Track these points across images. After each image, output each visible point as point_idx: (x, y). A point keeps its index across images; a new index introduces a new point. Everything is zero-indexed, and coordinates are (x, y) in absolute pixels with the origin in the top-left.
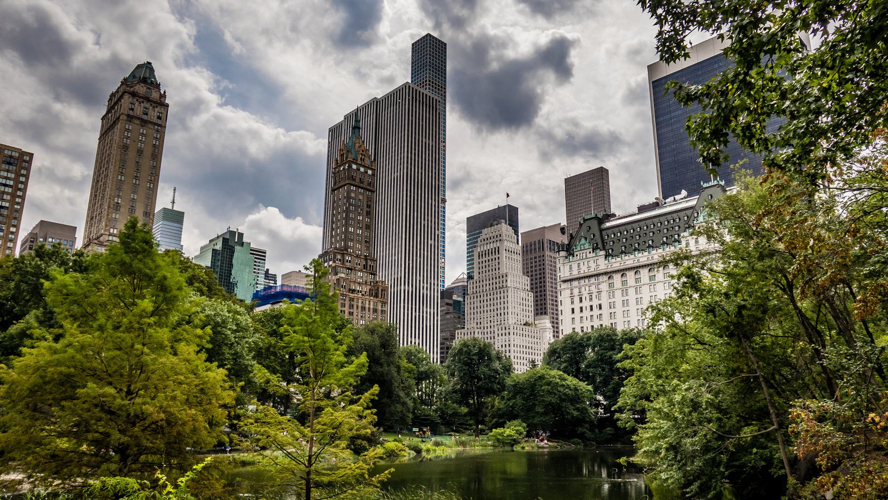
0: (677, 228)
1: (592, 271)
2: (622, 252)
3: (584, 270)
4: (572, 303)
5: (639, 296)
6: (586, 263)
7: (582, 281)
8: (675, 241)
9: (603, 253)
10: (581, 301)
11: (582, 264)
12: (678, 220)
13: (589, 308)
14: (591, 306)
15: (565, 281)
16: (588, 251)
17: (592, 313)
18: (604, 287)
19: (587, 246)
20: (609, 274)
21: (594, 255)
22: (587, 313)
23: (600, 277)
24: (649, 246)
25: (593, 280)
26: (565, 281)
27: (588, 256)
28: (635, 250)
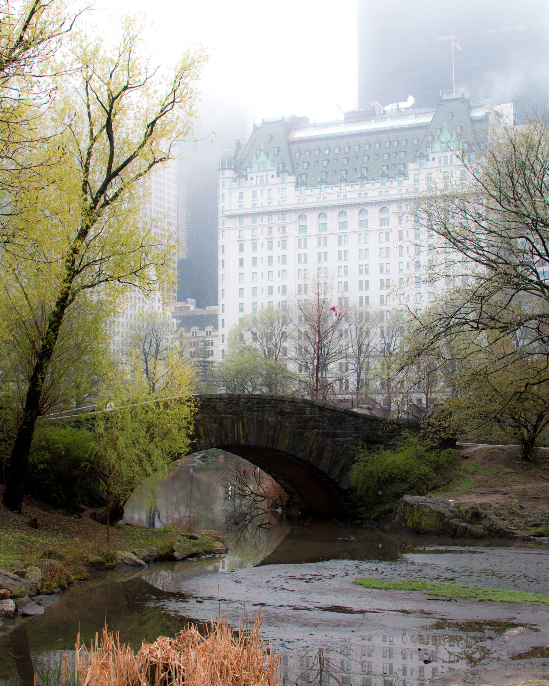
0: (402, 155)
1: (275, 206)
2: (322, 182)
3: (263, 202)
4: (241, 249)
5: (343, 248)
6: (266, 192)
7: (259, 219)
8: (400, 174)
9: (292, 179)
10: (254, 249)
11: (259, 193)
12: (404, 143)
13: (266, 260)
14: (270, 258)
15: (231, 217)
16: (270, 174)
17: (270, 268)
18: (292, 231)
19: (269, 165)
20: (301, 213)
21: (279, 180)
22: (263, 267)
23: (288, 216)
24: (362, 178)
25: (275, 218)
26: (231, 217)
27: (271, 181)
28: (342, 180)
